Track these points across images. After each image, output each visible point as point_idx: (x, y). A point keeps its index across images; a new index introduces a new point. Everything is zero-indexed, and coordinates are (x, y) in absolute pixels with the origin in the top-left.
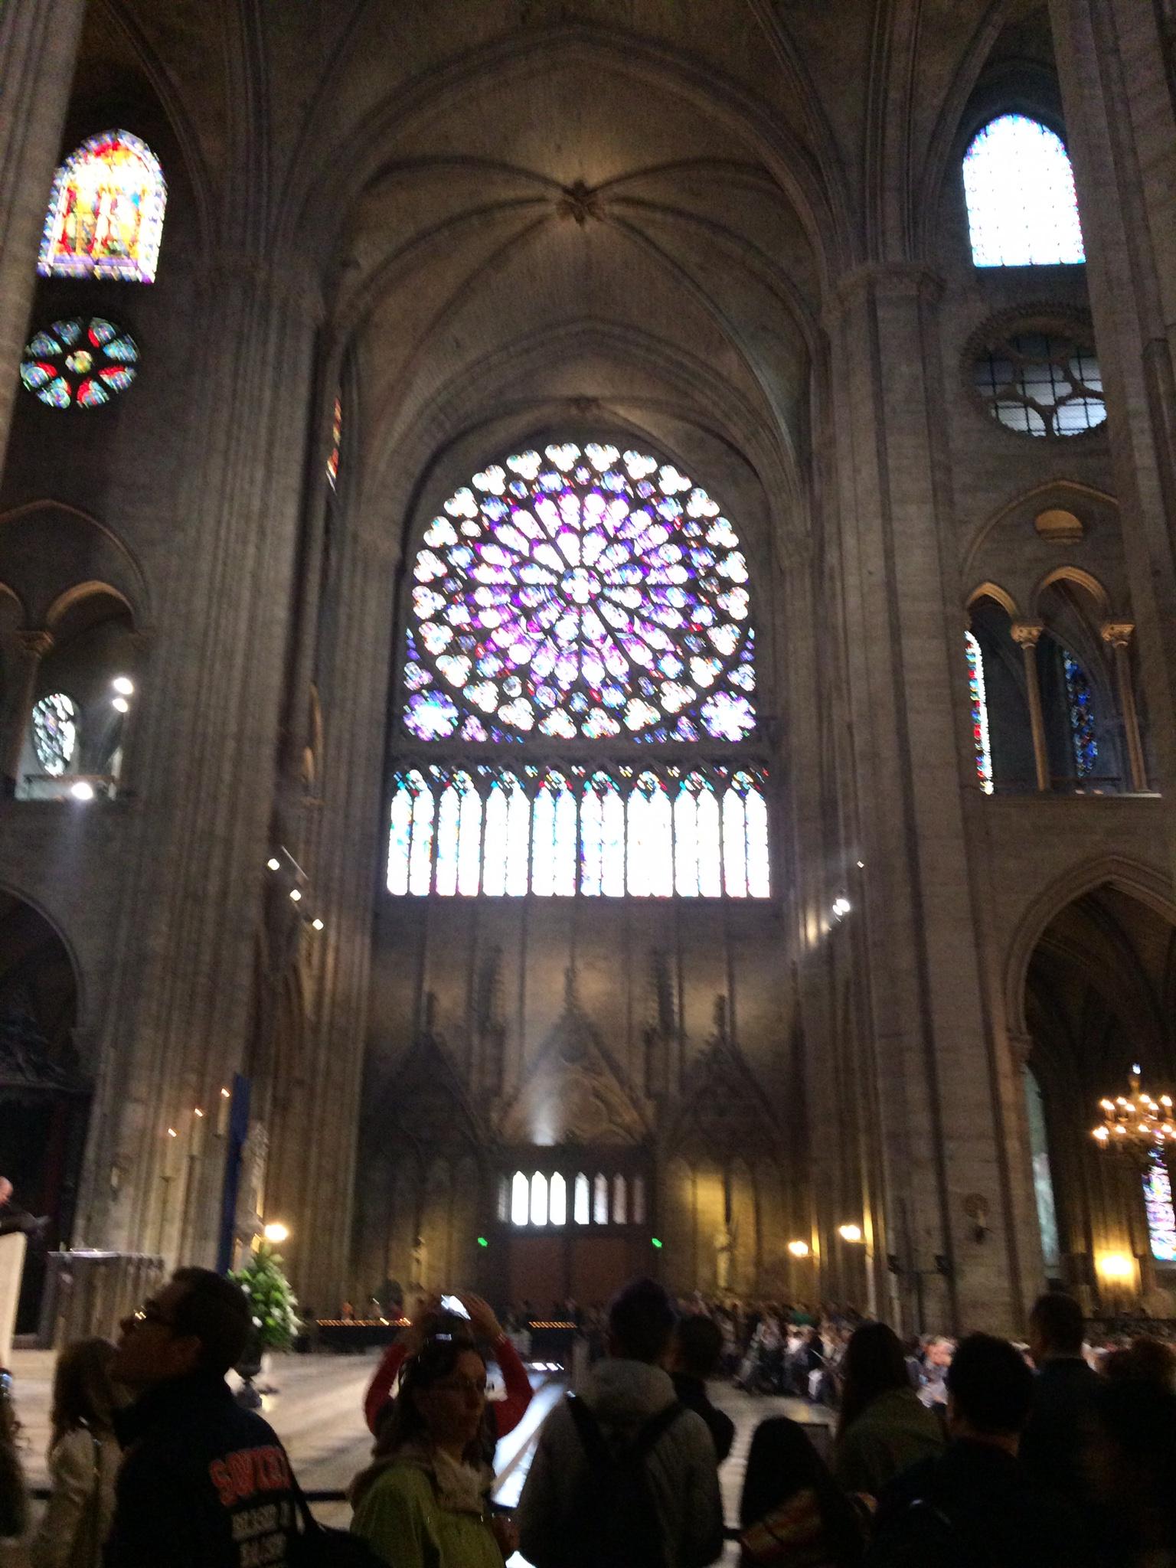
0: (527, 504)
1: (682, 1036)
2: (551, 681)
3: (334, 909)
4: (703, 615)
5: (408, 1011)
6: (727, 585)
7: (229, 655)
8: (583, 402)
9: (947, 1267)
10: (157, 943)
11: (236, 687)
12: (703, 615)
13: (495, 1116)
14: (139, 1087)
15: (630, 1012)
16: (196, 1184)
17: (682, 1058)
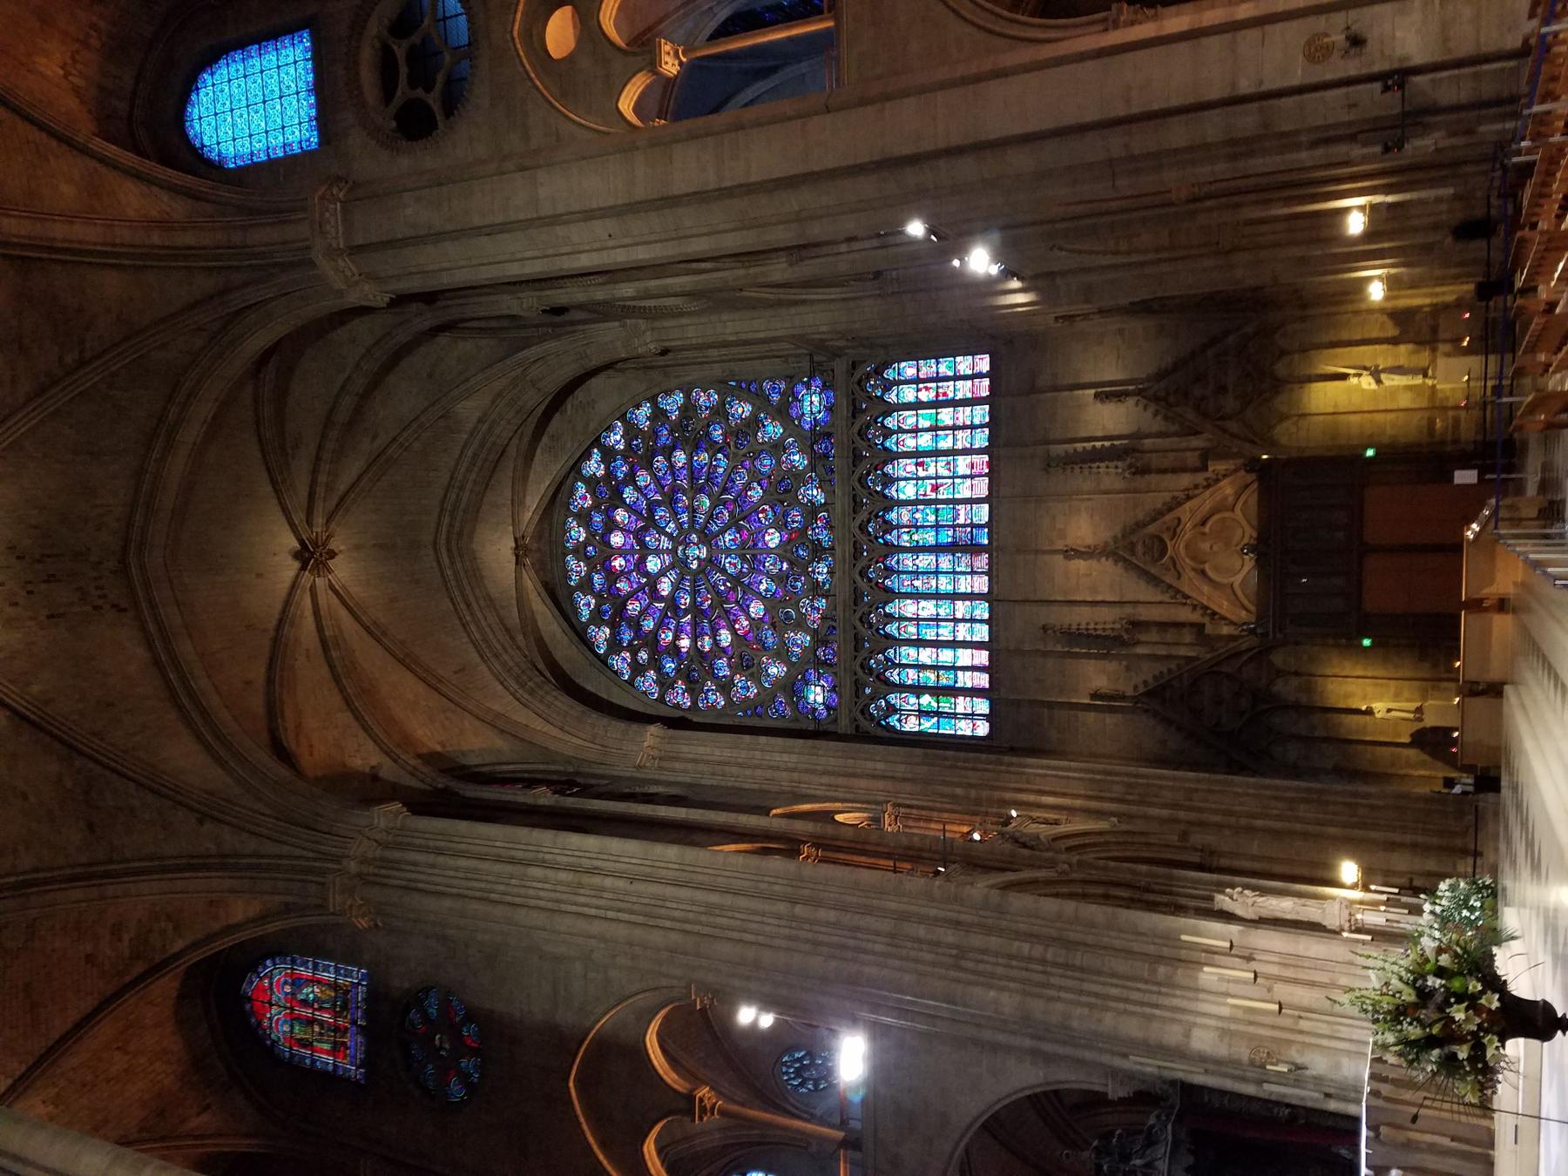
0: (621, 604)
1: (1137, 436)
2: (781, 579)
3: (997, 794)
4: (717, 434)
5: (1110, 719)
6: (688, 409)
7: (710, 909)
8: (520, 551)
9: (1397, 78)
10: (1008, 1003)
11: (743, 902)
12: (717, 434)
13: (1226, 630)
14: (1172, 1035)
15: (1106, 492)
16: (1289, 973)
17: (1160, 435)
